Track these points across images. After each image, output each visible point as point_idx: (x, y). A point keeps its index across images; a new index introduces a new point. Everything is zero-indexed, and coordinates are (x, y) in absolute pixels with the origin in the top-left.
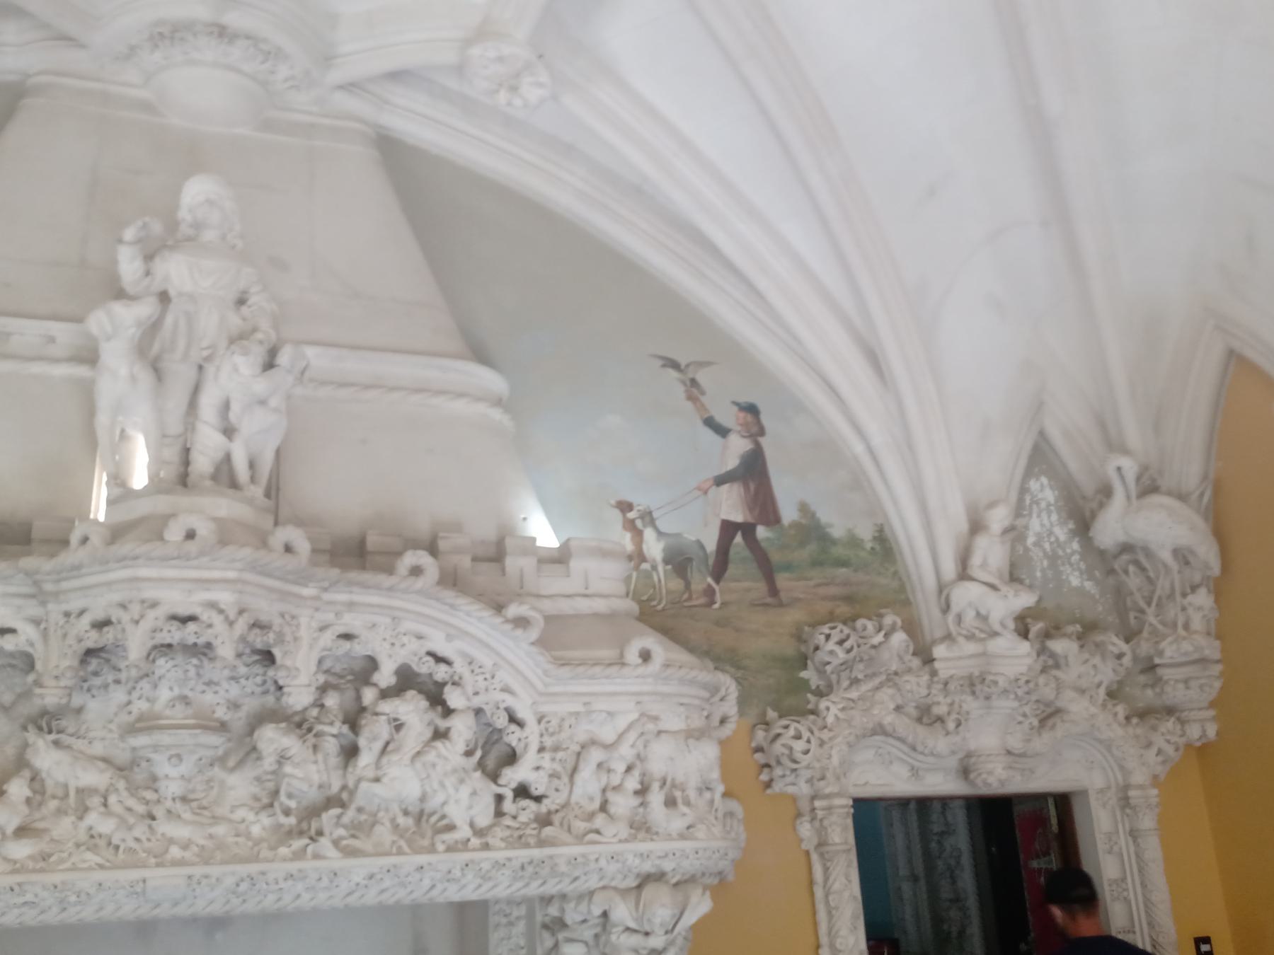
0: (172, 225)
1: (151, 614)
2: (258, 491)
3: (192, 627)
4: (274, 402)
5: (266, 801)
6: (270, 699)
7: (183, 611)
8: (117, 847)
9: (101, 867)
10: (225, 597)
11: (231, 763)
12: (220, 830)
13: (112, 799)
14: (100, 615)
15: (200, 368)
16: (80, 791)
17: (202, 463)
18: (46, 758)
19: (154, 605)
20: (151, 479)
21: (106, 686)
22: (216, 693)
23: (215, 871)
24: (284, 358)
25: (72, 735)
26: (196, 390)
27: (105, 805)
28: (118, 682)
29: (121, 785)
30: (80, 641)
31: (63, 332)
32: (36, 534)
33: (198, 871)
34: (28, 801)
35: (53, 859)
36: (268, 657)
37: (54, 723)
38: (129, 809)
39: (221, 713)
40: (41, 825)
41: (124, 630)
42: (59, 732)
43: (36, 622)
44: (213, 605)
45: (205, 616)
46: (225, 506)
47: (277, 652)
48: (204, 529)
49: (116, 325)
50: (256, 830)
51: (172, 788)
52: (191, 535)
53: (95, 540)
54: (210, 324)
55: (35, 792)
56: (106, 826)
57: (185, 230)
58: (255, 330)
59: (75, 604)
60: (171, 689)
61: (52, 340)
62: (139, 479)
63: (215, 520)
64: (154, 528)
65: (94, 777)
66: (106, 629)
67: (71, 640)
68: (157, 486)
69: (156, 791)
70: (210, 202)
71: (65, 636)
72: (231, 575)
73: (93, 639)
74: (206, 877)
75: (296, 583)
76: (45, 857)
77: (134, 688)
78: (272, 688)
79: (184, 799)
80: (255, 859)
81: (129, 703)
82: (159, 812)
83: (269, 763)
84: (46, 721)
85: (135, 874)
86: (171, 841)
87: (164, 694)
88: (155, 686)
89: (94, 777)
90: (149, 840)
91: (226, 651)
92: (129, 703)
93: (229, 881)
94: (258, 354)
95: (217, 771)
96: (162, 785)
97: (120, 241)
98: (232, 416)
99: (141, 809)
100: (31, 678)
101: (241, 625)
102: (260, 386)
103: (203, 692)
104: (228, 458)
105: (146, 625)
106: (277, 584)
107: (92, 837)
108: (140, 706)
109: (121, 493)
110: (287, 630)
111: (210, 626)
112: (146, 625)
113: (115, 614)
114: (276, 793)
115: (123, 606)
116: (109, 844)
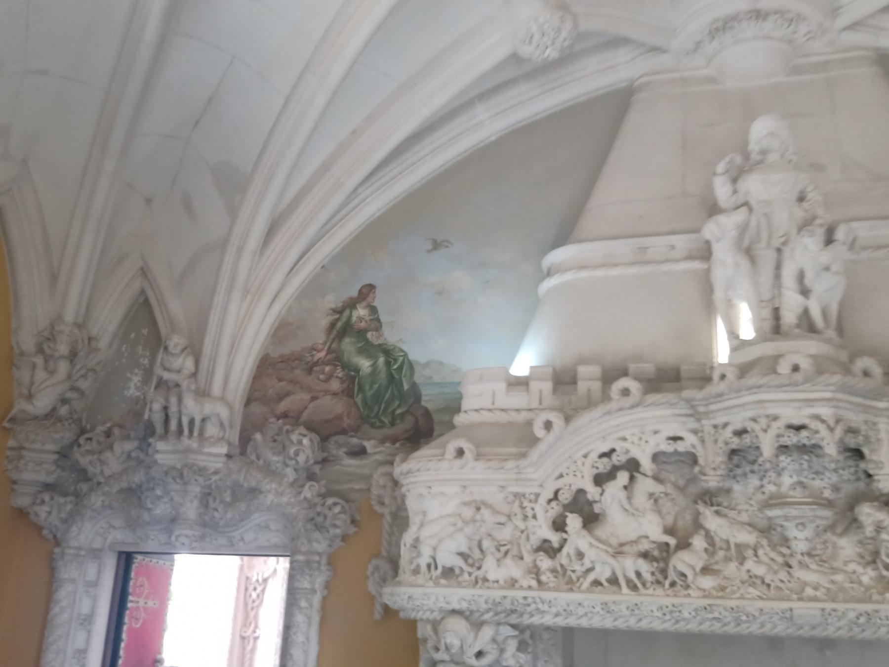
0: (746, 155)
1: (775, 425)
2: (831, 333)
3: (804, 433)
4: (835, 268)
5: (869, 558)
6: (861, 485)
7: (797, 422)
8: (769, 586)
9: (761, 598)
10: (825, 411)
11: (839, 530)
12: (839, 578)
13: (760, 552)
14: (738, 426)
15: (779, 250)
16: (738, 546)
17: (789, 317)
18: (712, 522)
19: (775, 418)
20: (756, 331)
21: (745, 475)
22: (822, 479)
23: (841, 607)
24: (840, 234)
25: (726, 507)
26: (778, 266)
27: (756, 555)
28: (753, 472)
29: (765, 542)
30: (727, 443)
31: (682, 242)
32: (684, 375)
33: (829, 606)
34: (706, 550)
35: (728, 590)
36: (858, 454)
37: (714, 499)
38: (772, 560)
39: (827, 494)
40: (716, 567)
41: (757, 437)
42: (719, 505)
43: (695, 432)
44: (817, 417)
45: (814, 424)
46: (812, 346)
47: (866, 451)
48: (805, 364)
49: (721, 231)
50: (865, 579)
51: (801, 546)
52: (796, 368)
53: (731, 376)
54: (784, 218)
55: (709, 544)
56: (760, 570)
57: (755, 157)
58: (814, 218)
59: (720, 420)
60: (791, 477)
61: (673, 247)
62: (747, 332)
63: (811, 356)
64: (771, 364)
65: (747, 537)
66: (744, 436)
67: (721, 444)
68: (762, 337)
69: (789, 548)
70: (771, 134)
71: (716, 441)
72: (828, 395)
73: (735, 442)
74: (834, 610)
75: (874, 399)
76: (723, 589)
77: (764, 476)
78: (863, 476)
79: (809, 555)
80: (869, 600)
81: (762, 486)
82: (793, 562)
83: (869, 531)
84: (709, 497)
85: (785, 605)
86: (806, 584)
87: (787, 481)
88: (779, 475)
89: (747, 537)
90: (789, 582)
91: (831, 450)
92: (762, 486)
93: (852, 615)
94: (820, 233)
95: (829, 536)
96: (793, 544)
97: (715, 174)
98: (807, 282)
99: (780, 560)
100: (697, 469)
101: (839, 431)
102: (826, 256)
103: (813, 479)
104: (806, 312)
105: (772, 432)
106: (859, 400)
107: (751, 577)
108: (770, 488)
109: (738, 346)
110: (871, 433)
111: (817, 432)
112: (772, 432)
113: (750, 425)
114: (876, 554)
115: (754, 420)
116: (763, 582)
